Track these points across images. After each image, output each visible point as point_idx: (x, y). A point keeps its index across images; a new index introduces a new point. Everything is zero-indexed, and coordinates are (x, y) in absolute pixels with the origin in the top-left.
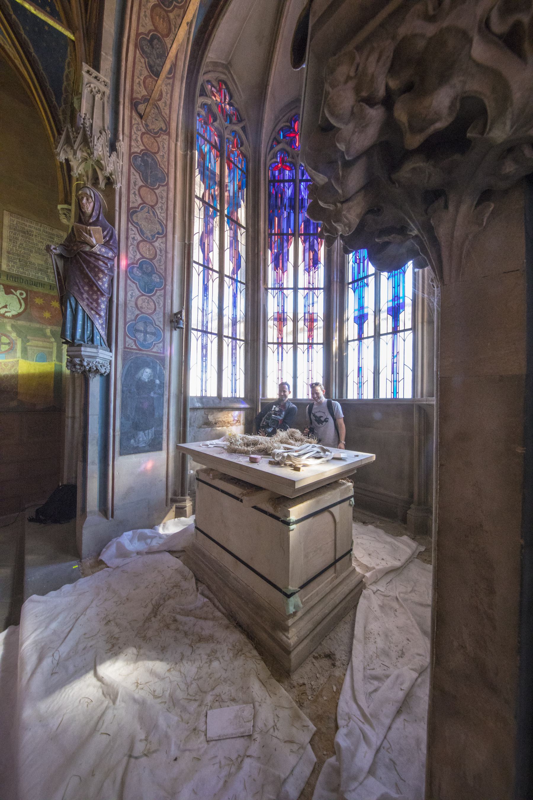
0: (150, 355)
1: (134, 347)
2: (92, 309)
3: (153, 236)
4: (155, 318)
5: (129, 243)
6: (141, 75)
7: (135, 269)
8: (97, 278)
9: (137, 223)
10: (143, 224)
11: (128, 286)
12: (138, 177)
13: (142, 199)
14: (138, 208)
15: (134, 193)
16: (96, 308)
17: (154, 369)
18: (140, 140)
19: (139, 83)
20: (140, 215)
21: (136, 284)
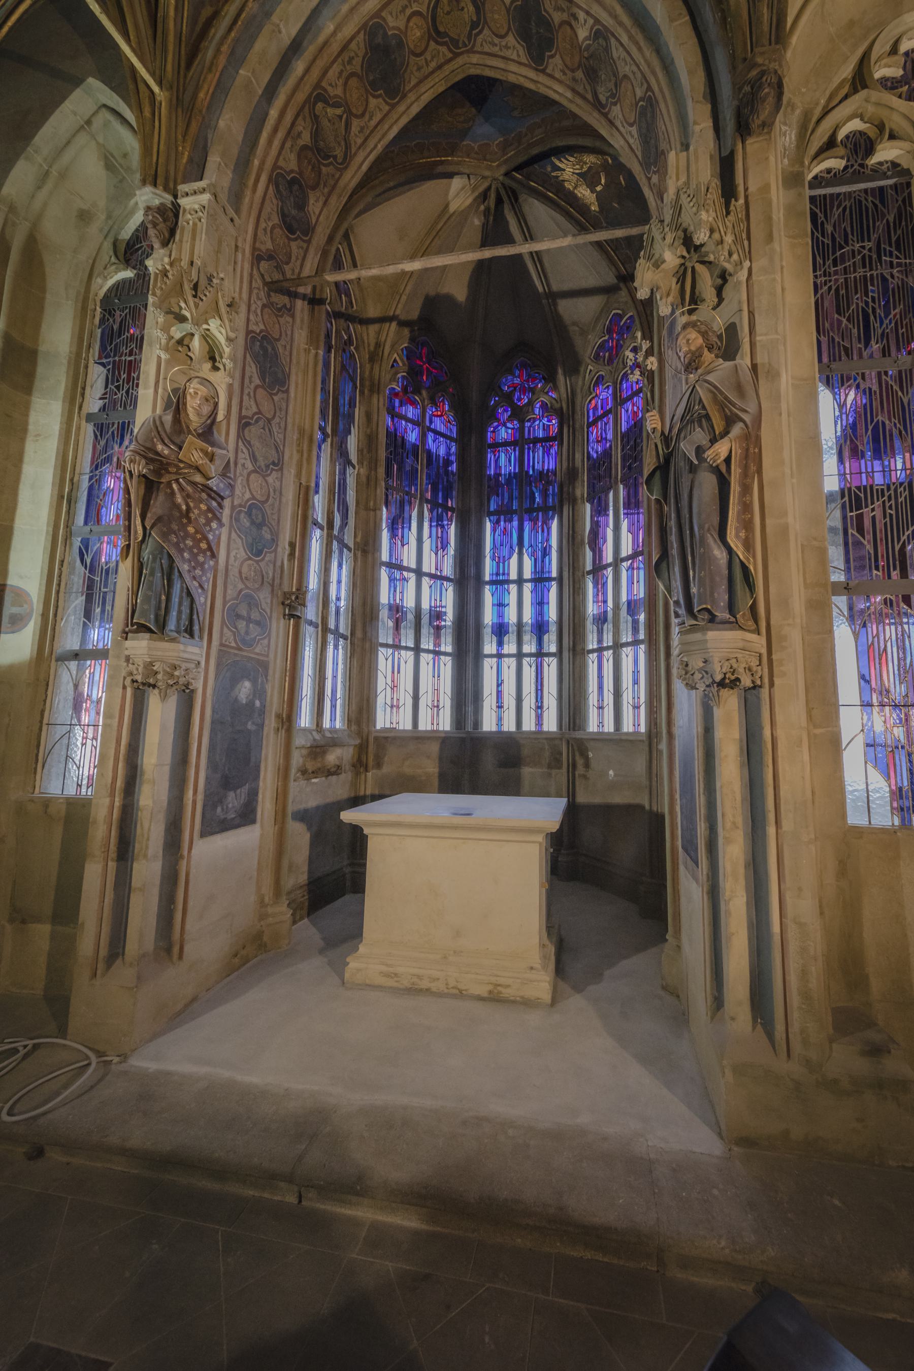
0: (252, 658)
1: (233, 644)
2: (194, 578)
3: (267, 466)
4: (262, 597)
5: (238, 471)
6: (269, 219)
7: (242, 515)
8: (208, 528)
9: (249, 443)
10: (256, 444)
11: (232, 542)
12: (254, 371)
13: (257, 405)
14: (252, 418)
15: (249, 394)
16: (201, 576)
17: (254, 682)
18: (259, 314)
19: (265, 230)
20: (253, 429)
21: (242, 539)
